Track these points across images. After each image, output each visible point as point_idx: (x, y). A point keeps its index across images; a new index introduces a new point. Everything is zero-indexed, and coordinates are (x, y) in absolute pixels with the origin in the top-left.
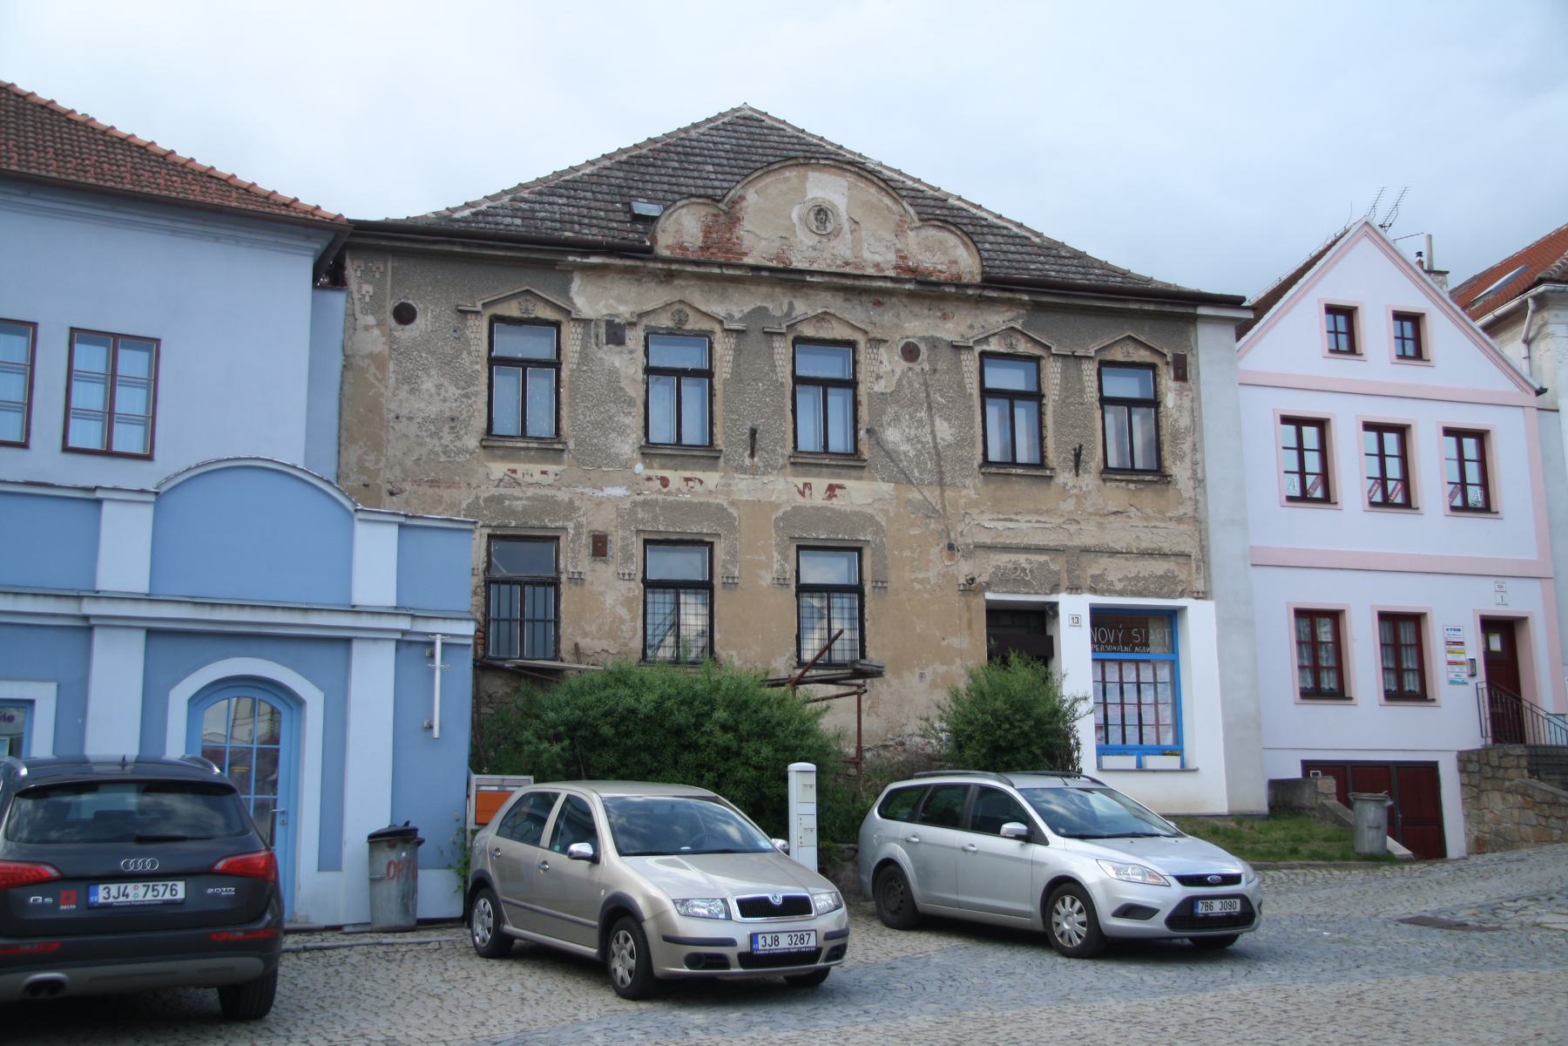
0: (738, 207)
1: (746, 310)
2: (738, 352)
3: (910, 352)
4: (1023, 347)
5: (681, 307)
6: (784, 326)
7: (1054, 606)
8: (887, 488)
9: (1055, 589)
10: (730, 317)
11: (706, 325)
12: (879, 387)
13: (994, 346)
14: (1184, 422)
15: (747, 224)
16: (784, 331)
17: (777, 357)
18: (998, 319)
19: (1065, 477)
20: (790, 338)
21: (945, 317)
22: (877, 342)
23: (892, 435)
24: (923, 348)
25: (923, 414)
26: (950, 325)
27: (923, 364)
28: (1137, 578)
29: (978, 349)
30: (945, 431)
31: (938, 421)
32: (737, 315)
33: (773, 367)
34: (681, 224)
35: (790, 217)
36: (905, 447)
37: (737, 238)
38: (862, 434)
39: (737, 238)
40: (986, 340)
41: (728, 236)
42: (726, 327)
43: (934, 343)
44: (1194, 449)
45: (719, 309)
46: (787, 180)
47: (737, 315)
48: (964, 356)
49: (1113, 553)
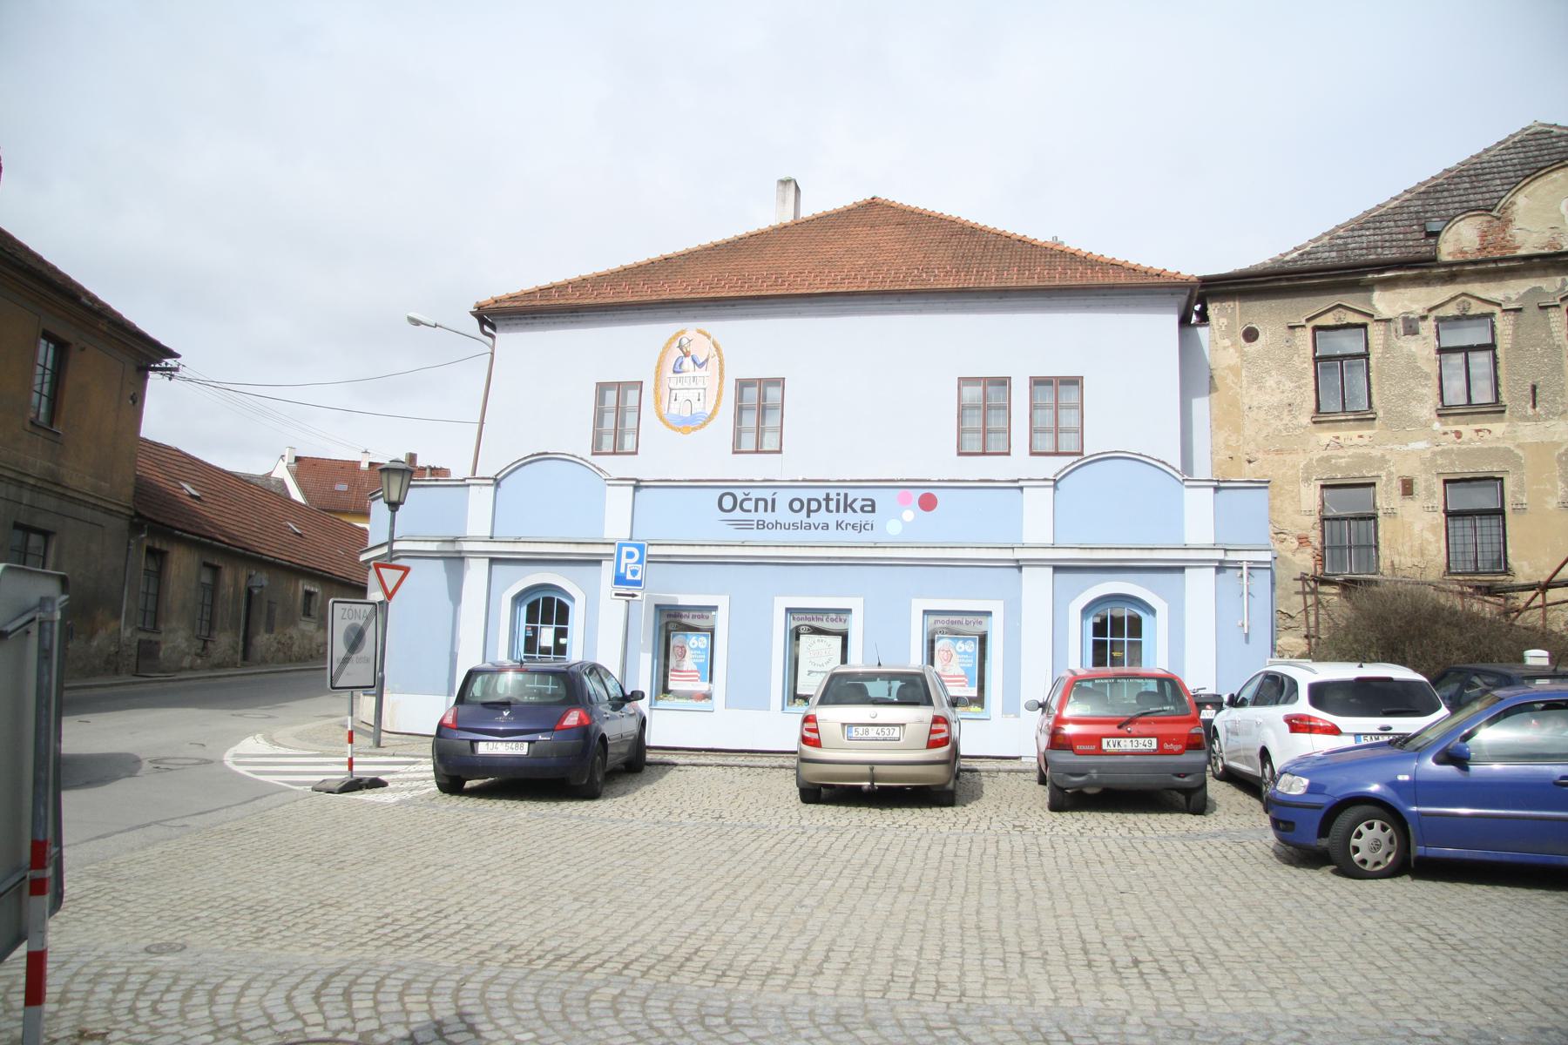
0: (1509, 211)
1: (1522, 291)
2: (1516, 326)
5: (1463, 298)
6: (1558, 299)
10: (1508, 299)
11: (1487, 309)
15: (1517, 224)
16: (1558, 303)
17: (1553, 325)
32: (1514, 297)
33: (1550, 334)
34: (1460, 234)
35: (1559, 210)
37: (1510, 236)
39: (1510, 236)
41: (1502, 236)
42: (1504, 308)
46: (1555, 180)
47: (1514, 297)
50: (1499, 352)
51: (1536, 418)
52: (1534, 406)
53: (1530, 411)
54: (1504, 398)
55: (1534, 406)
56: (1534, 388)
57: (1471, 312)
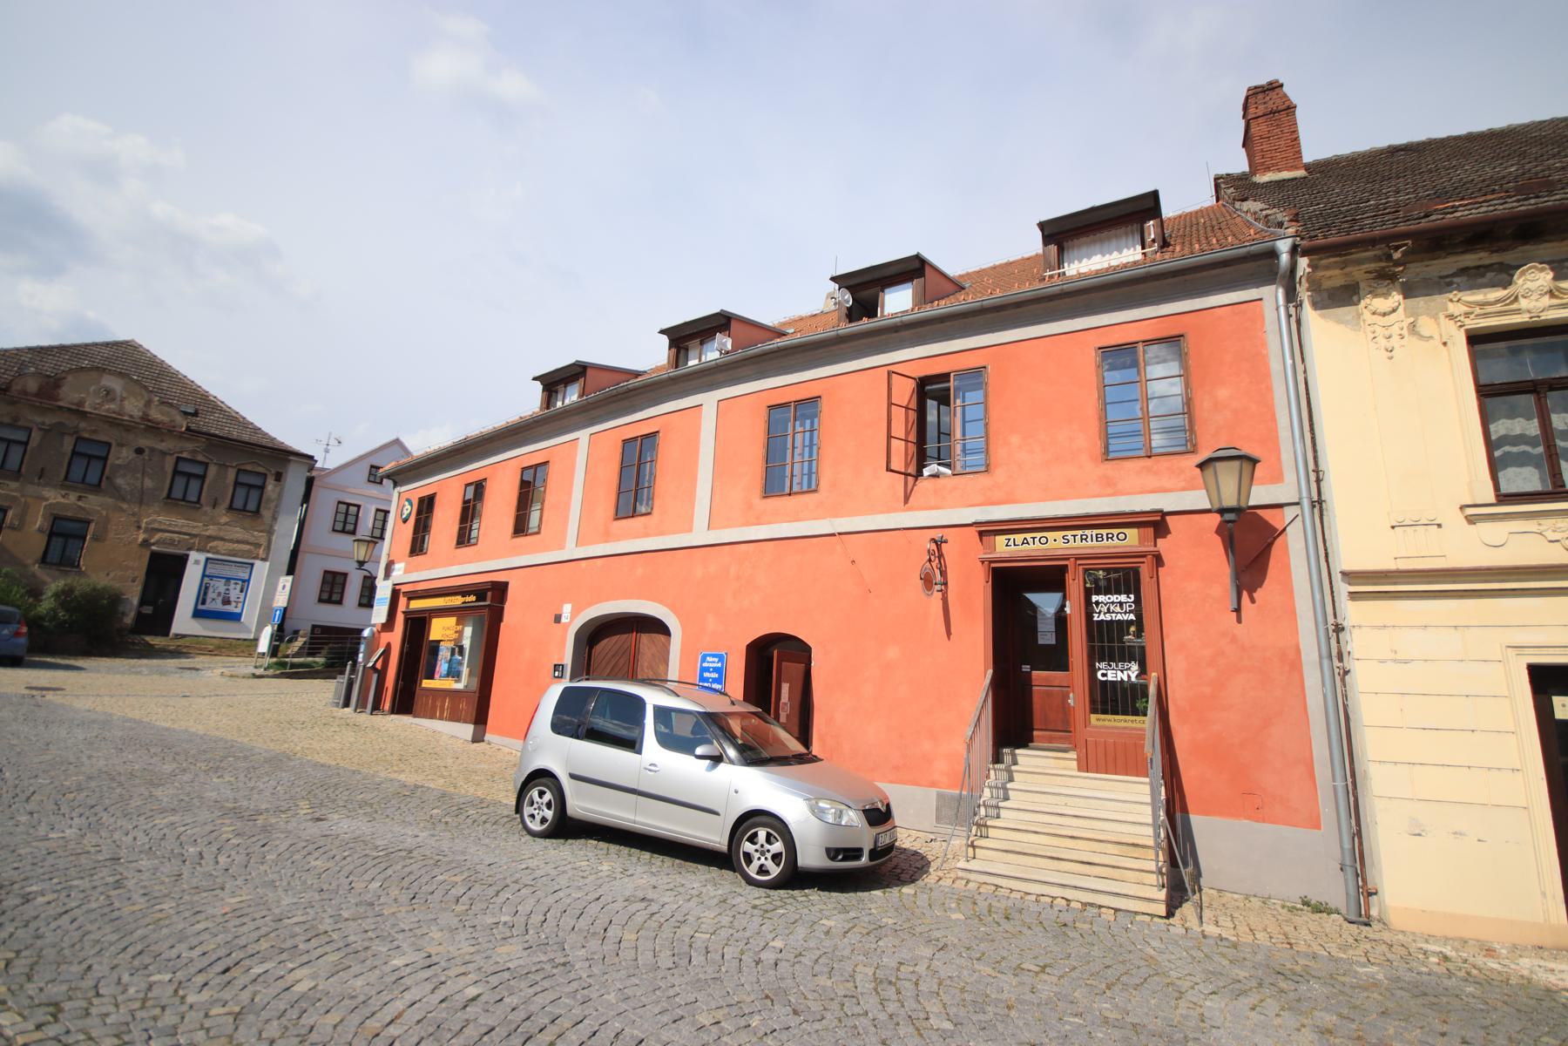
3: (139, 451)
4: (200, 458)
7: (187, 556)
8: (110, 501)
9: (190, 549)
12: (117, 462)
13: (184, 455)
14: (274, 496)
18: (190, 446)
19: (208, 509)
20: (75, 436)
21: (162, 441)
22: (121, 445)
23: (119, 481)
24: (147, 451)
25: (139, 475)
26: (164, 444)
27: (146, 456)
28: (234, 550)
29: (176, 455)
30: (148, 483)
31: (146, 480)
36: (124, 487)
38: (104, 478)
40: (181, 452)
43: (152, 450)
44: (277, 506)
45: (39, 419)
48: (168, 458)
49: (222, 539)
50: (29, 448)
51: (39, 485)
52: (40, 478)
53: (36, 481)
54: (23, 470)
55: (40, 478)
56: (42, 470)
57: (19, 423)
